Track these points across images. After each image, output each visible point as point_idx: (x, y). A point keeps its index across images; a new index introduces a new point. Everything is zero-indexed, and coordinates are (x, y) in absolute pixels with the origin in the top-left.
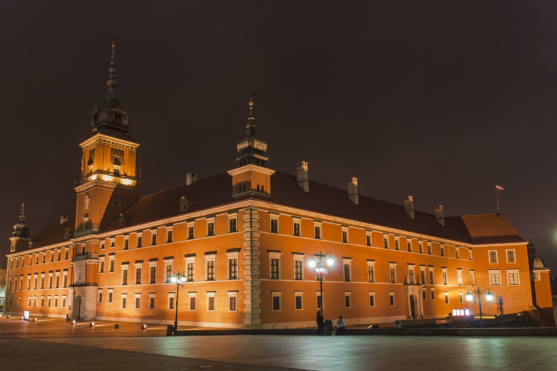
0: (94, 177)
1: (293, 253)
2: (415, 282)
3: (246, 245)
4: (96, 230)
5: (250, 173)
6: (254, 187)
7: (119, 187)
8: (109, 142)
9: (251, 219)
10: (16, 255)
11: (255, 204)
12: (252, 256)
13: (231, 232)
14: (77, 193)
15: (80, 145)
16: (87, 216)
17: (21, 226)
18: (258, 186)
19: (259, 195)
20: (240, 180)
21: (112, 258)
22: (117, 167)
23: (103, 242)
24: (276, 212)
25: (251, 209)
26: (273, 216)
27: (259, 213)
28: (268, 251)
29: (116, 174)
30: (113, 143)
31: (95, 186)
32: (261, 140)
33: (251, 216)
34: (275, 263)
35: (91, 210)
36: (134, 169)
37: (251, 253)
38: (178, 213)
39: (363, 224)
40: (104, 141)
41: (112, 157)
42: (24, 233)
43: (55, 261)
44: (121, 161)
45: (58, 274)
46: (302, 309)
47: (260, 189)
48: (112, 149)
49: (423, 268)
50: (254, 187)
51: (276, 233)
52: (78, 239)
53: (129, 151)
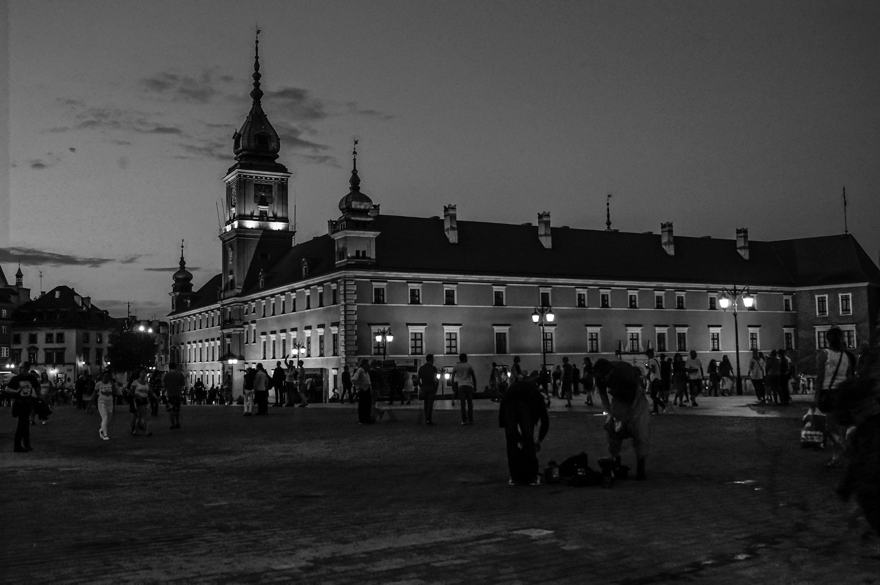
1: (408, 324)
2: (642, 349)
3: (342, 319)
4: (239, 291)
7: (268, 233)
8: (251, 177)
9: (345, 290)
12: (345, 331)
16: (231, 273)
18: (358, 252)
19: (360, 262)
20: (341, 246)
21: (254, 325)
23: (246, 307)
24: (383, 280)
26: (376, 285)
29: (263, 217)
30: (256, 177)
38: (300, 279)
39: (533, 279)
40: (245, 176)
41: (256, 196)
45: (212, 343)
47: (361, 255)
49: (658, 330)
52: (225, 302)
53: (279, 185)
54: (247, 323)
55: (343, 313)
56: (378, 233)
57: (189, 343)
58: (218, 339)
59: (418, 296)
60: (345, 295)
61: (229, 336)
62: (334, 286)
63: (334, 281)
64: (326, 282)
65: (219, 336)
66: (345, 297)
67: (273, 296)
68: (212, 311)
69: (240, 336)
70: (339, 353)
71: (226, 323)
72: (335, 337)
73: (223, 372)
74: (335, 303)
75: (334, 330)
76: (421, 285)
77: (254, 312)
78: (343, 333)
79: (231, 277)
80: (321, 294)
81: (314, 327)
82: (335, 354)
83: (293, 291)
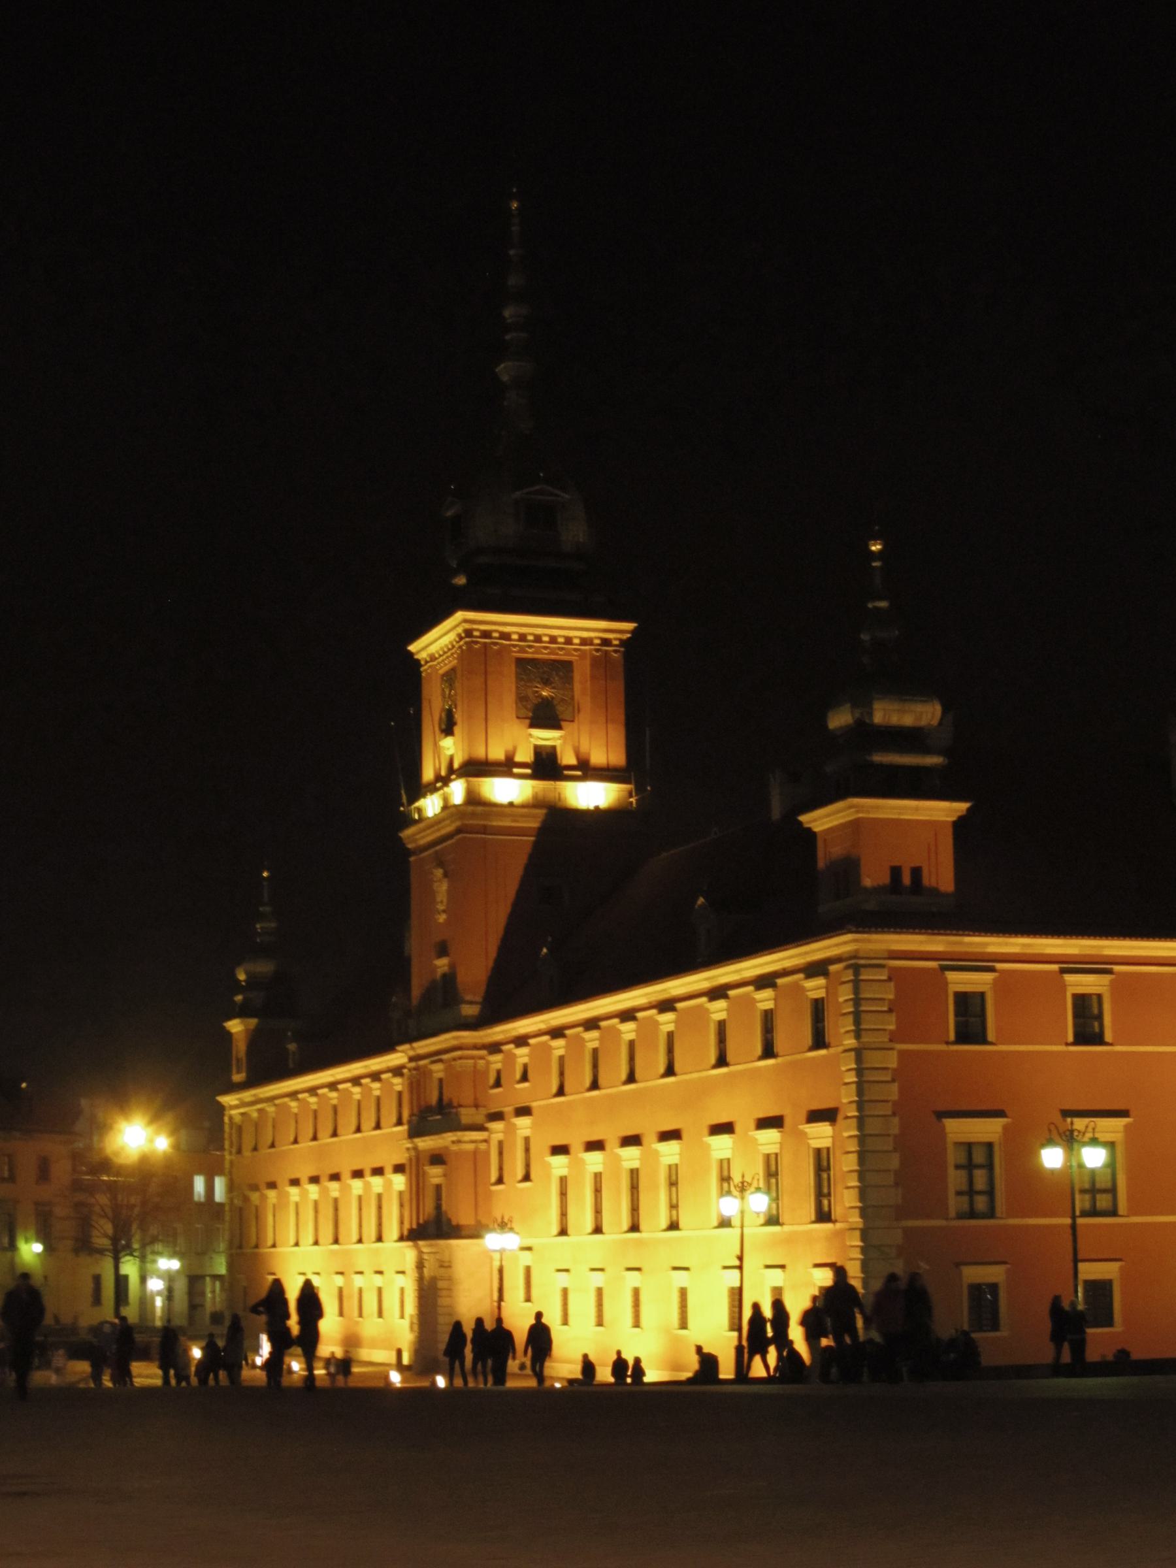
0: (457, 791)
3: (846, 1098)
5: (855, 826)
6: (873, 877)
7: (559, 821)
8: (506, 636)
9: (857, 1001)
10: (248, 1095)
11: (871, 946)
12: (862, 1139)
13: (812, 1049)
14: (409, 853)
15: (412, 648)
16: (443, 950)
17: (265, 967)
18: (896, 872)
20: (837, 851)
21: (523, 1122)
22: (545, 737)
23: (496, 1061)
24: (982, 962)
25: (856, 964)
26: (961, 981)
27: (895, 976)
28: (942, 1115)
30: (522, 637)
31: (459, 831)
32: (907, 687)
33: (856, 990)
34: (976, 1158)
35: (458, 931)
36: (618, 735)
37: (861, 1126)
40: (486, 634)
41: (521, 699)
42: (269, 1004)
43: (325, 1139)
44: (560, 708)
45: (377, 1183)
46: (1003, 1333)
47: (907, 880)
48: (523, 665)
50: (873, 877)
51: (984, 1041)
53: (595, 662)
54: (498, 1116)
55: (852, 1078)
56: (962, 807)
57: (295, 1182)
58: (399, 1169)
59: (1100, 1017)
60: (857, 1016)
61: (437, 1159)
62: (815, 987)
63: (815, 969)
64: (785, 973)
65: (401, 1158)
66: (857, 1022)
67: (591, 1024)
68: (375, 1076)
69: (477, 1159)
70: (837, 1212)
71: (431, 1113)
72: (822, 1162)
73: (420, 1279)
74: (819, 1042)
75: (821, 1134)
76: (1106, 979)
77: (525, 1078)
78: (853, 1146)
79: (442, 964)
80: (768, 1018)
81: (744, 1124)
82: (823, 1216)
83: (666, 1006)
